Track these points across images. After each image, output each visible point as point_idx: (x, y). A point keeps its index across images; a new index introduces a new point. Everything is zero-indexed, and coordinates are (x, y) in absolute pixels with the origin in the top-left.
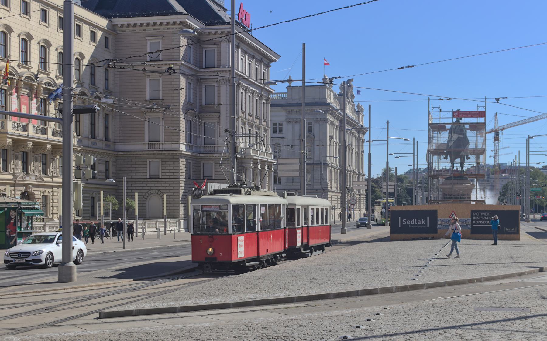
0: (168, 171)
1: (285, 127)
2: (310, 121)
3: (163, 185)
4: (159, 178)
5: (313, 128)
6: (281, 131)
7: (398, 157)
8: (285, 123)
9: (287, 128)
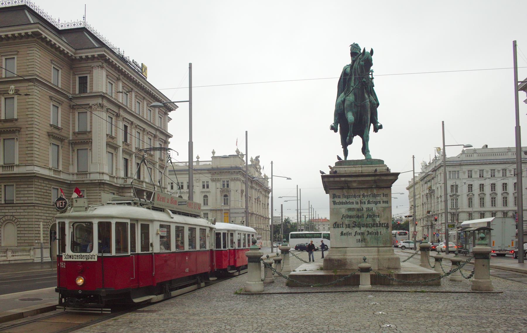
0: (23, 195)
3: (18, 211)
4: (13, 203)
6: (208, 187)
7: (287, 201)
9: (212, 185)
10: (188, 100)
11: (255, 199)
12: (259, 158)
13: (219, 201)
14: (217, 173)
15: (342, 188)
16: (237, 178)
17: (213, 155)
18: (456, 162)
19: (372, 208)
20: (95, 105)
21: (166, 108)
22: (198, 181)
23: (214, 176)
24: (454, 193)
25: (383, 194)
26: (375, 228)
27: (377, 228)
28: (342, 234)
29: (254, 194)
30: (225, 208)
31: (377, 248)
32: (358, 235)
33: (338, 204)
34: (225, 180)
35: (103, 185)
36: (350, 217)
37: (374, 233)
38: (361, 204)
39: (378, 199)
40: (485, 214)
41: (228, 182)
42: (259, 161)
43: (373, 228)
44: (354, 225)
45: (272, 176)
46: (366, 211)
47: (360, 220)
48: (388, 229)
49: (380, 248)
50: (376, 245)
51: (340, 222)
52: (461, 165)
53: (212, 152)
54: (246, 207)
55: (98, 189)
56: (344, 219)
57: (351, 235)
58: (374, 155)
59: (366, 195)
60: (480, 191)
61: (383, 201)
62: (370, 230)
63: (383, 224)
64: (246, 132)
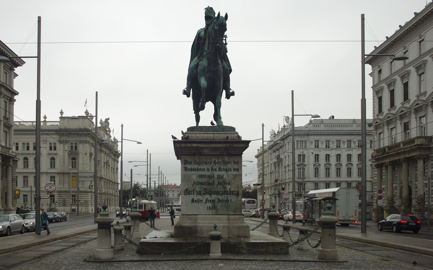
5: (78, 147)
6: (55, 149)
7: (137, 166)
8: (58, 142)
10: (37, 56)
11: (104, 163)
12: (109, 121)
13: (66, 164)
14: (65, 134)
15: (194, 155)
16: (86, 140)
17: (61, 115)
18: (303, 132)
19: (223, 175)
21: (12, 63)
22: (44, 142)
23: (62, 137)
24: (302, 163)
25: (234, 162)
26: (226, 196)
27: (227, 196)
28: (193, 201)
29: (103, 158)
30: (72, 171)
31: (227, 216)
32: (209, 202)
33: (189, 170)
34: (74, 143)
36: (201, 184)
37: (224, 200)
38: (212, 171)
39: (229, 166)
40: (330, 184)
41: (76, 144)
42: (109, 124)
43: (224, 195)
44: (205, 192)
45: (122, 139)
46: (217, 178)
47: (211, 187)
48: (239, 197)
49: (231, 216)
50: (226, 213)
51: (191, 188)
52: (308, 135)
53: (60, 112)
54: (95, 171)
56: (195, 185)
57: (202, 202)
58: (226, 122)
59: (217, 162)
60: (326, 161)
61: (234, 169)
62: (221, 197)
63: (233, 191)
64: (97, 93)
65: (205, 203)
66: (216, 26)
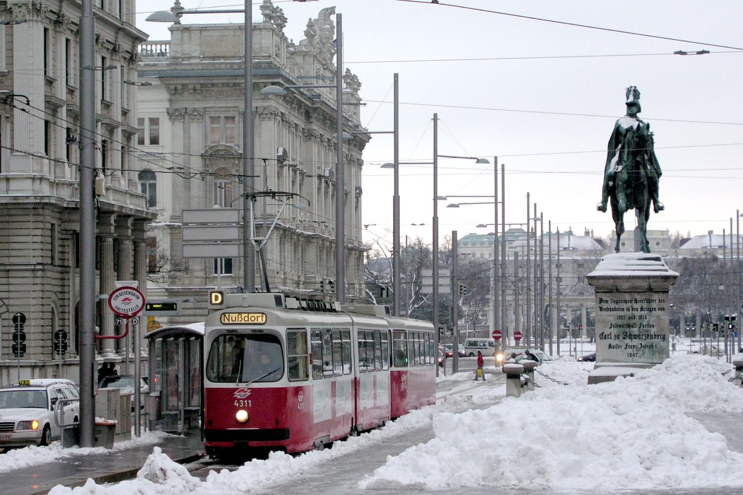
1: (166, 130)
2: (230, 114)
8: (166, 117)
15: (610, 292)
20: (20, 7)
27: (654, 340)
28: (610, 346)
34: (222, 115)
35: (43, 208)
36: (620, 326)
39: (654, 305)
45: (436, 156)
51: (607, 331)
55: (31, 218)
56: (612, 328)
63: (658, 335)
64: (396, 76)
65: (626, 348)
66: (636, 137)
